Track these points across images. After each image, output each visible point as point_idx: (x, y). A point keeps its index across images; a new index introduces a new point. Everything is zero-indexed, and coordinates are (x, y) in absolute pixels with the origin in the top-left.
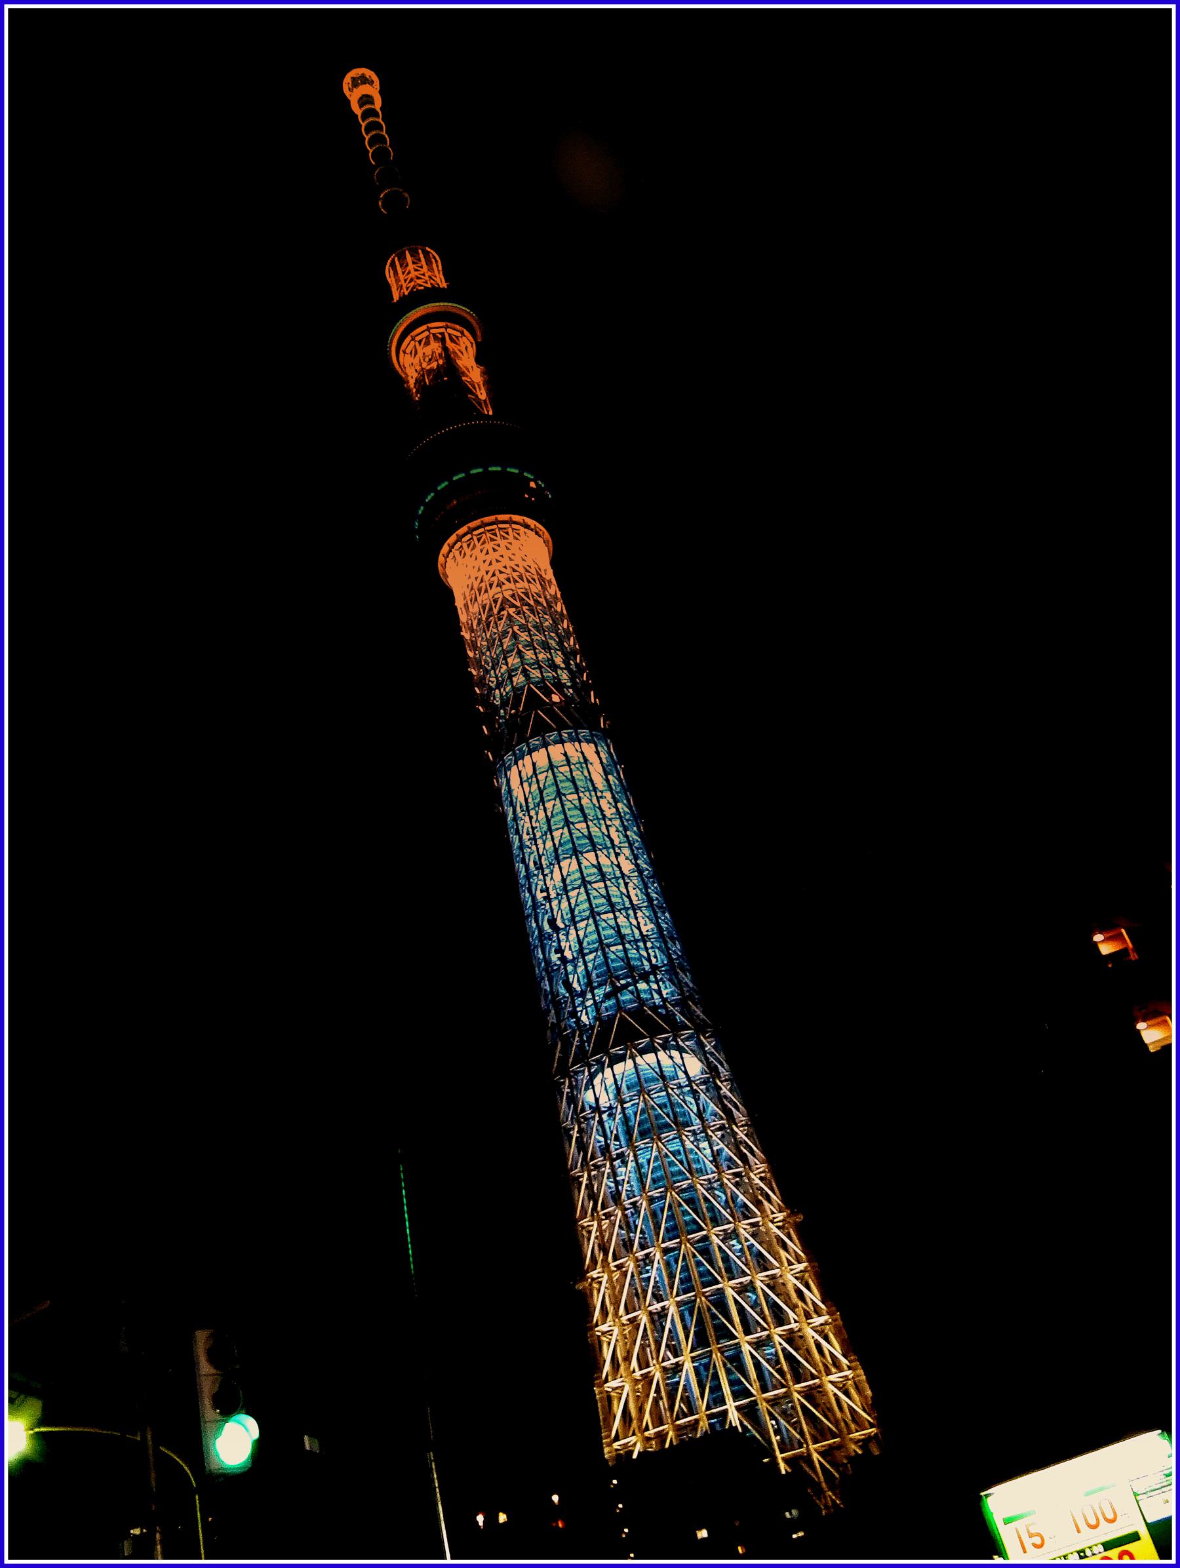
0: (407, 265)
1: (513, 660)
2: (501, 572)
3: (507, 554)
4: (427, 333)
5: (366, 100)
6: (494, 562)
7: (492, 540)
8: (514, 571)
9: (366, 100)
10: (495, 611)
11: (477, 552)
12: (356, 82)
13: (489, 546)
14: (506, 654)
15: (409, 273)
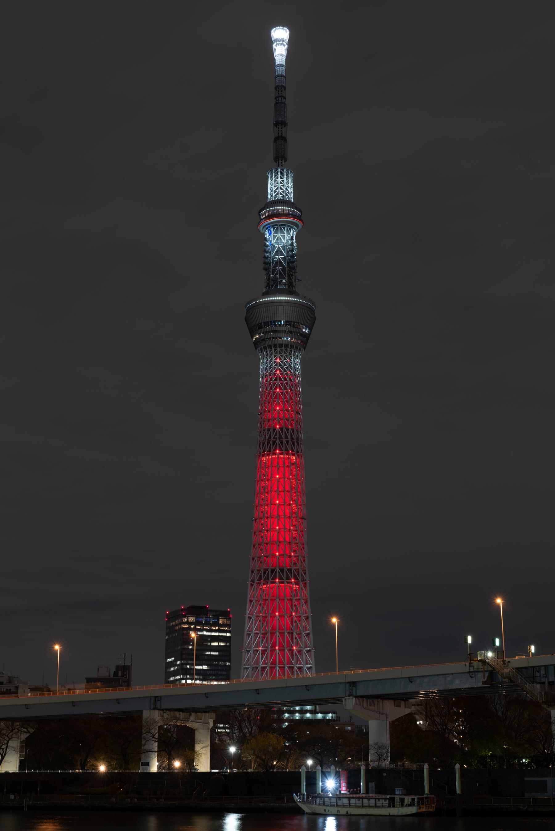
0: (278, 178)
3: (284, 361)
15: (277, 183)
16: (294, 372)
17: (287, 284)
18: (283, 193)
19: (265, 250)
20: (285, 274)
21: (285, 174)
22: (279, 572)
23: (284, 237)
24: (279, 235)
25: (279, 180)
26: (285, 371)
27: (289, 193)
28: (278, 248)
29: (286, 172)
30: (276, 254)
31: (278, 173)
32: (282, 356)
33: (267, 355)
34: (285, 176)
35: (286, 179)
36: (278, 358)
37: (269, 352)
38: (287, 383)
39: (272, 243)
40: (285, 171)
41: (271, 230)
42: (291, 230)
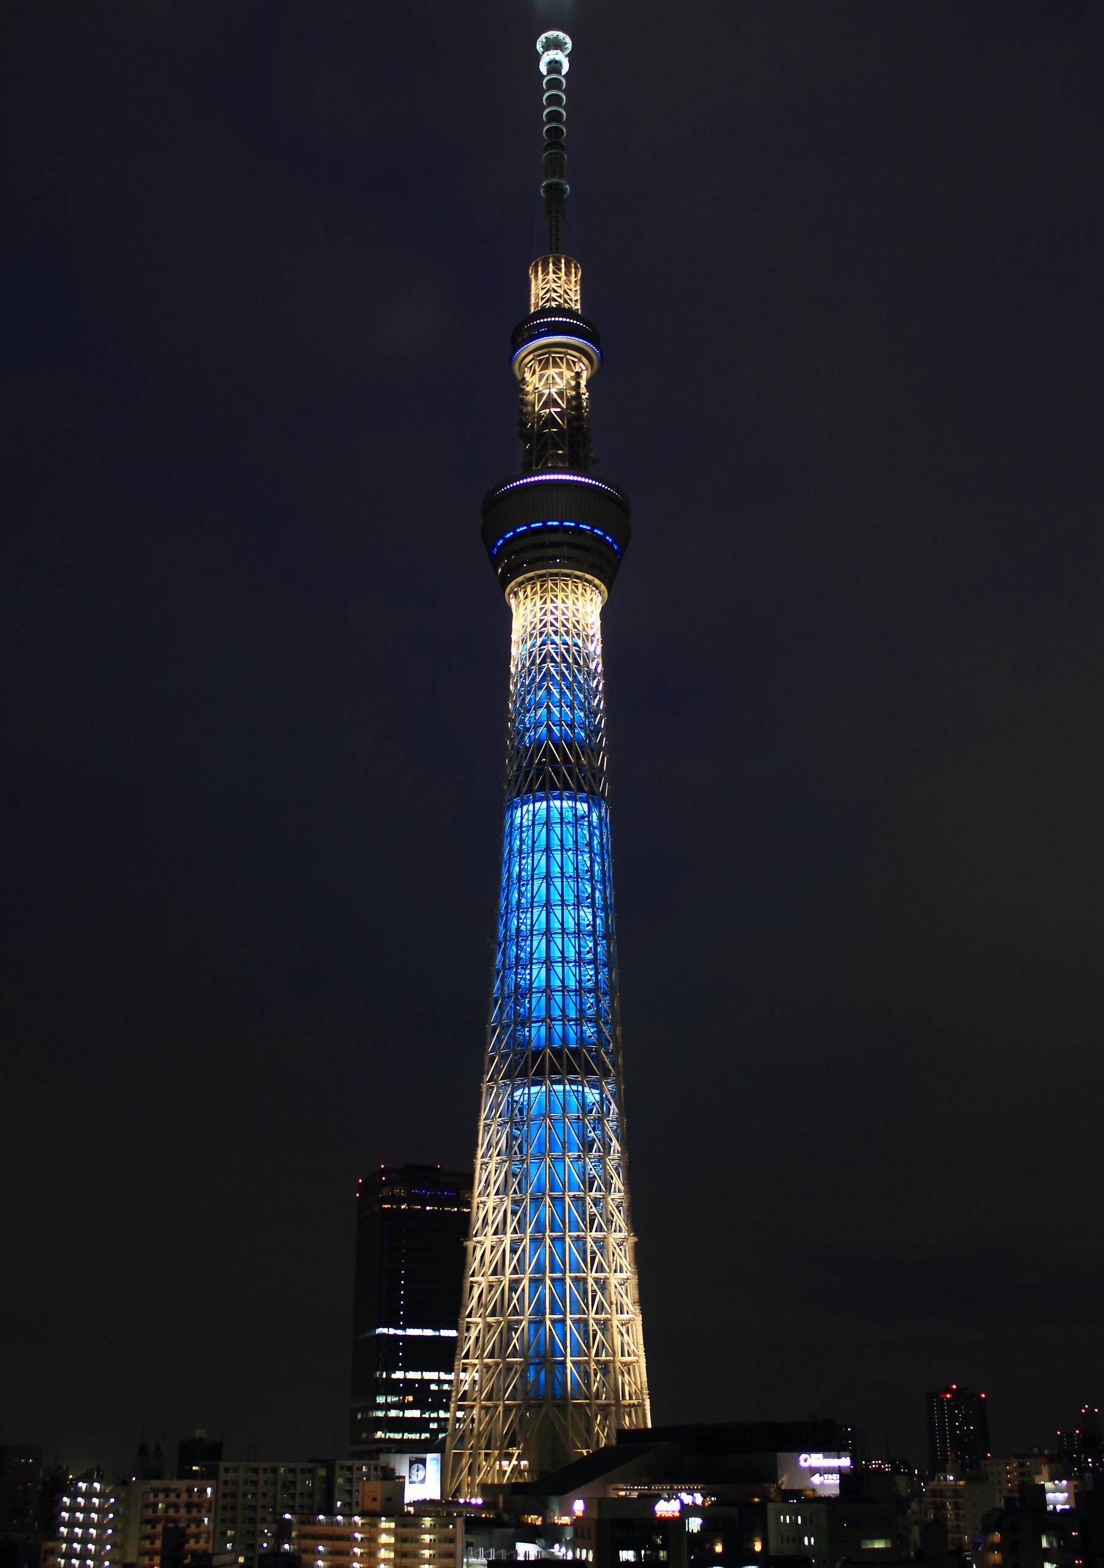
0: (548, 274)
1: (543, 712)
2: (552, 625)
3: (561, 606)
4: (547, 355)
5: (554, 66)
6: (549, 613)
7: (552, 590)
8: (564, 625)
9: (554, 66)
10: (538, 662)
11: (537, 597)
12: (547, 47)
13: (550, 595)
14: (539, 705)
15: (547, 283)
16: (584, 629)
21: (563, 266)
22: (550, 1057)
23: (561, 375)
24: (552, 371)
25: (552, 276)
30: (545, 406)
35: (566, 275)
36: (549, 601)
38: (568, 650)
39: (536, 386)
41: (535, 367)
42: (577, 364)
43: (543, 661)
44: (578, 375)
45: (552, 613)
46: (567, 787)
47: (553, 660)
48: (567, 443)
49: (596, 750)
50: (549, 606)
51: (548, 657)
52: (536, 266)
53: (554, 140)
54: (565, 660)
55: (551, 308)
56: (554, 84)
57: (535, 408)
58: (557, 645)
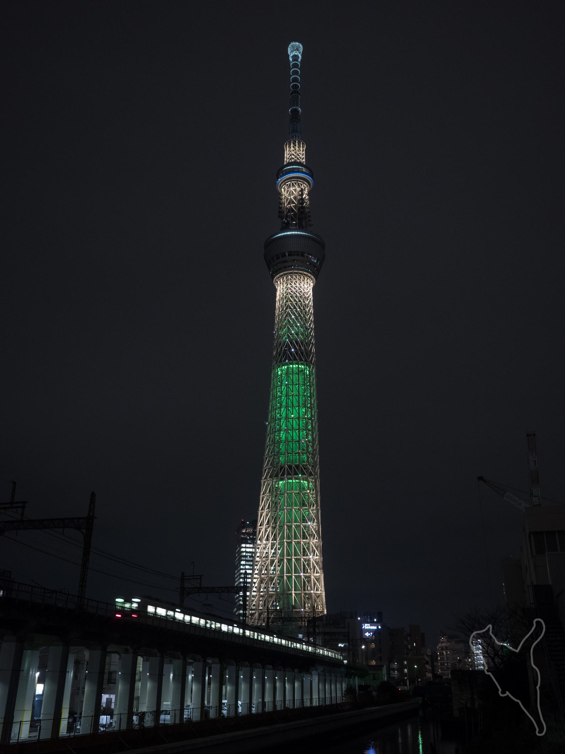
0: (291, 148)
2: (290, 294)
3: (294, 286)
9: (295, 57)
15: (290, 151)
16: (304, 295)
17: (297, 225)
18: (295, 158)
19: (280, 202)
20: (296, 219)
21: (297, 144)
24: (292, 189)
25: (292, 149)
26: (295, 293)
27: (300, 158)
28: (290, 198)
29: (298, 143)
30: (289, 203)
31: (291, 143)
32: (292, 282)
33: (281, 283)
34: (297, 146)
36: (289, 284)
37: (281, 280)
40: (297, 142)
43: (287, 309)
44: (302, 190)
45: (290, 289)
46: (295, 359)
47: (290, 308)
48: (297, 218)
49: (308, 344)
50: (289, 286)
51: (288, 307)
52: (286, 145)
53: (294, 90)
54: (295, 308)
55: (292, 162)
56: (295, 66)
57: (285, 205)
58: (292, 302)
